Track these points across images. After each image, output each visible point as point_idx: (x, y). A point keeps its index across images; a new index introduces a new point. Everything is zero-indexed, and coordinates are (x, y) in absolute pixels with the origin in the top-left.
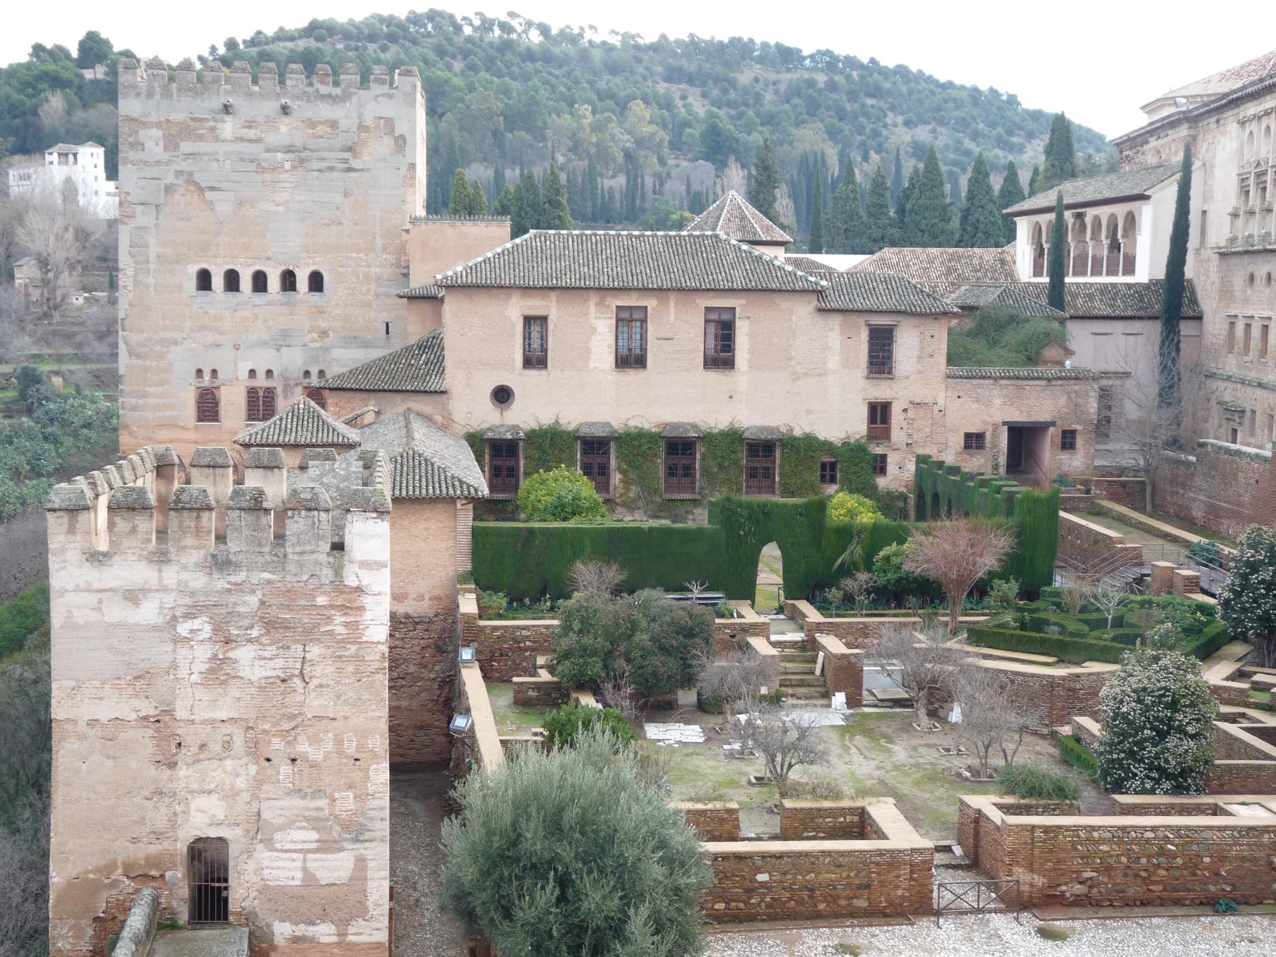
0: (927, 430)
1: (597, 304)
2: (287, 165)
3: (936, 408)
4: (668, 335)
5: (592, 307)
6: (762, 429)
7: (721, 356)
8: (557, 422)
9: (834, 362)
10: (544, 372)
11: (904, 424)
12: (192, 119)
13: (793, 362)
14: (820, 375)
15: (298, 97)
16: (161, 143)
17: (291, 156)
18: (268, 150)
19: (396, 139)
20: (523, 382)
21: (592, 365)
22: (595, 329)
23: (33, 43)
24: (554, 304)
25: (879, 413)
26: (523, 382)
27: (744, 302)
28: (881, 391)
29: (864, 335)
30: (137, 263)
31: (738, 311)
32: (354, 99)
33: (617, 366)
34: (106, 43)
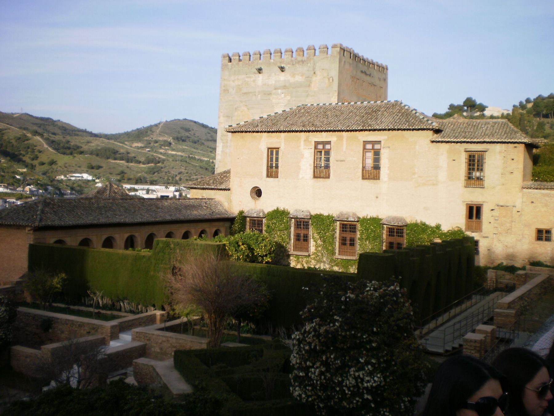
0: (508, 225)
1: (305, 141)
2: (283, 95)
3: (515, 210)
4: (342, 158)
5: (302, 143)
6: (394, 218)
7: (372, 173)
8: (278, 209)
9: (443, 176)
10: (277, 179)
11: (492, 220)
12: (248, 77)
13: (416, 176)
14: (434, 185)
15: (289, 64)
16: (235, 89)
17: (284, 91)
18: (276, 89)
19: (329, 79)
20: (265, 184)
21: (301, 176)
22: (303, 155)
23: (450, 104)
24: (283, 140)
25: (474, 212)
26: (265, 184)
27: (386, 137)
28: (475, 196)
29: (463, 159)
30: (223, 143)
31: (382, 143)
32: (312, 62)
33: (315, 177)
34: (474, 101)
